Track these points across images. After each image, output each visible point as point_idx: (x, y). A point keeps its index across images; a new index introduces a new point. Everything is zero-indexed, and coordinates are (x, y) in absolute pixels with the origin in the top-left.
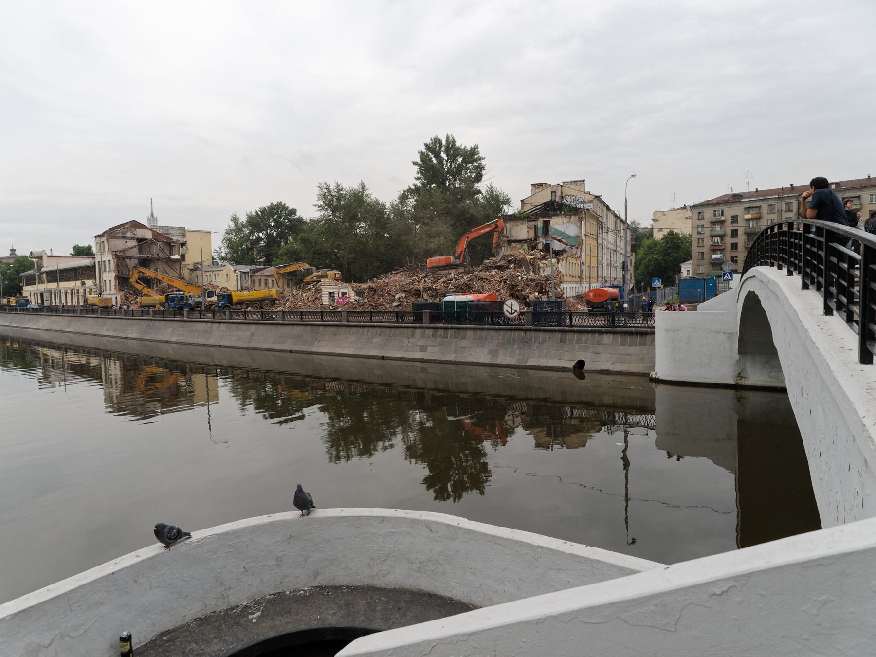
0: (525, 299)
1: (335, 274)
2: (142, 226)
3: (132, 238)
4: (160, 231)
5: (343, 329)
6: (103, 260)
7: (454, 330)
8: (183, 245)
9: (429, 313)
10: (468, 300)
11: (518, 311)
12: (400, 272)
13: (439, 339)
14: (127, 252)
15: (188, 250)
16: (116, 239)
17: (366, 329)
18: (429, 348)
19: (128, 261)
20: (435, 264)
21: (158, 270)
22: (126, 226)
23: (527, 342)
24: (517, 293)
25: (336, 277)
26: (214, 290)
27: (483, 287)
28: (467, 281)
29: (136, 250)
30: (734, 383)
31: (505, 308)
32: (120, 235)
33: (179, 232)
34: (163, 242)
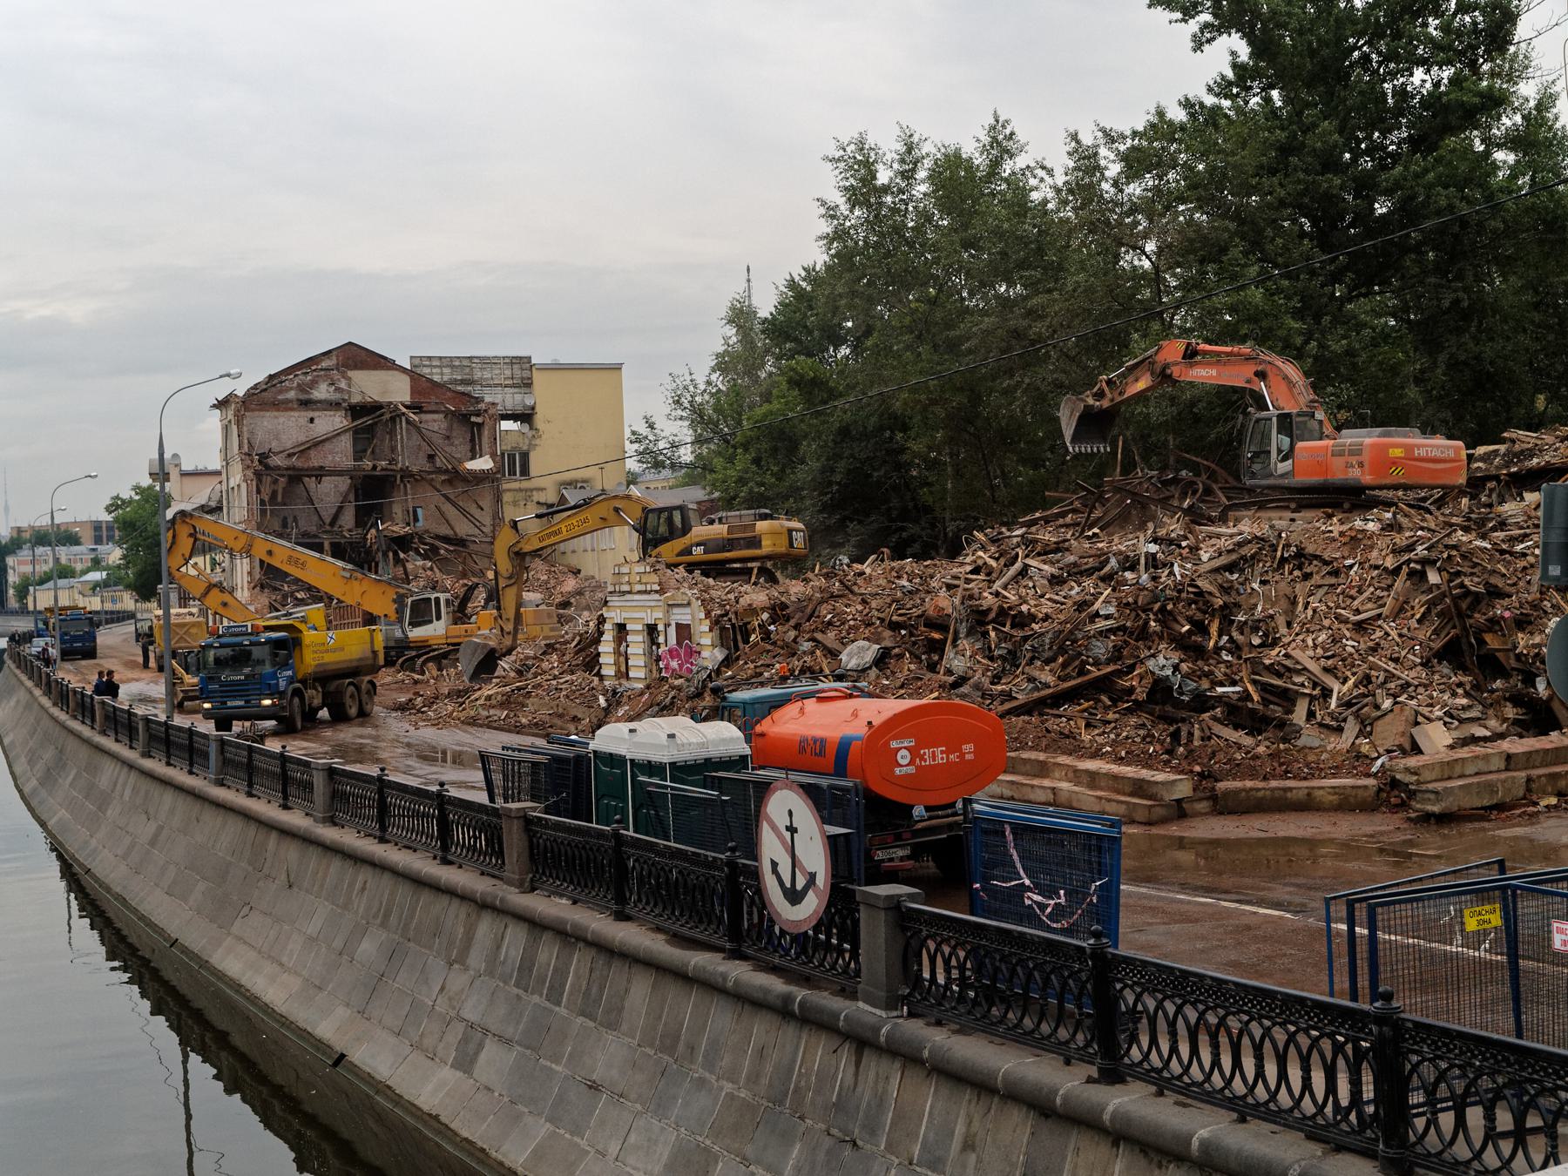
0: (1530, 680)
1: (790, 531)
2: (378, 362)
3: (333, 405)
4: (442, 374)
6: (231, 485)
7: (593, 952)
8: (526, 417)
9: (528, 822)
10: (641, 755)
11: (821, 881)
12: (1063, 515)
13: (536, 999)
14: (312, 453)
17: (365, 874)
19: (311, 483)
21: (419, 511)
22: (324, 365)
23: (855, 1144)
24: (1488, 638)
26: (433, 597)
27: (1293, 602)
28: (1216, 570)
29: (346, 443)
31: (771, 847)
32: (292, 395)
33: (508, 373)
34: (447, 413)
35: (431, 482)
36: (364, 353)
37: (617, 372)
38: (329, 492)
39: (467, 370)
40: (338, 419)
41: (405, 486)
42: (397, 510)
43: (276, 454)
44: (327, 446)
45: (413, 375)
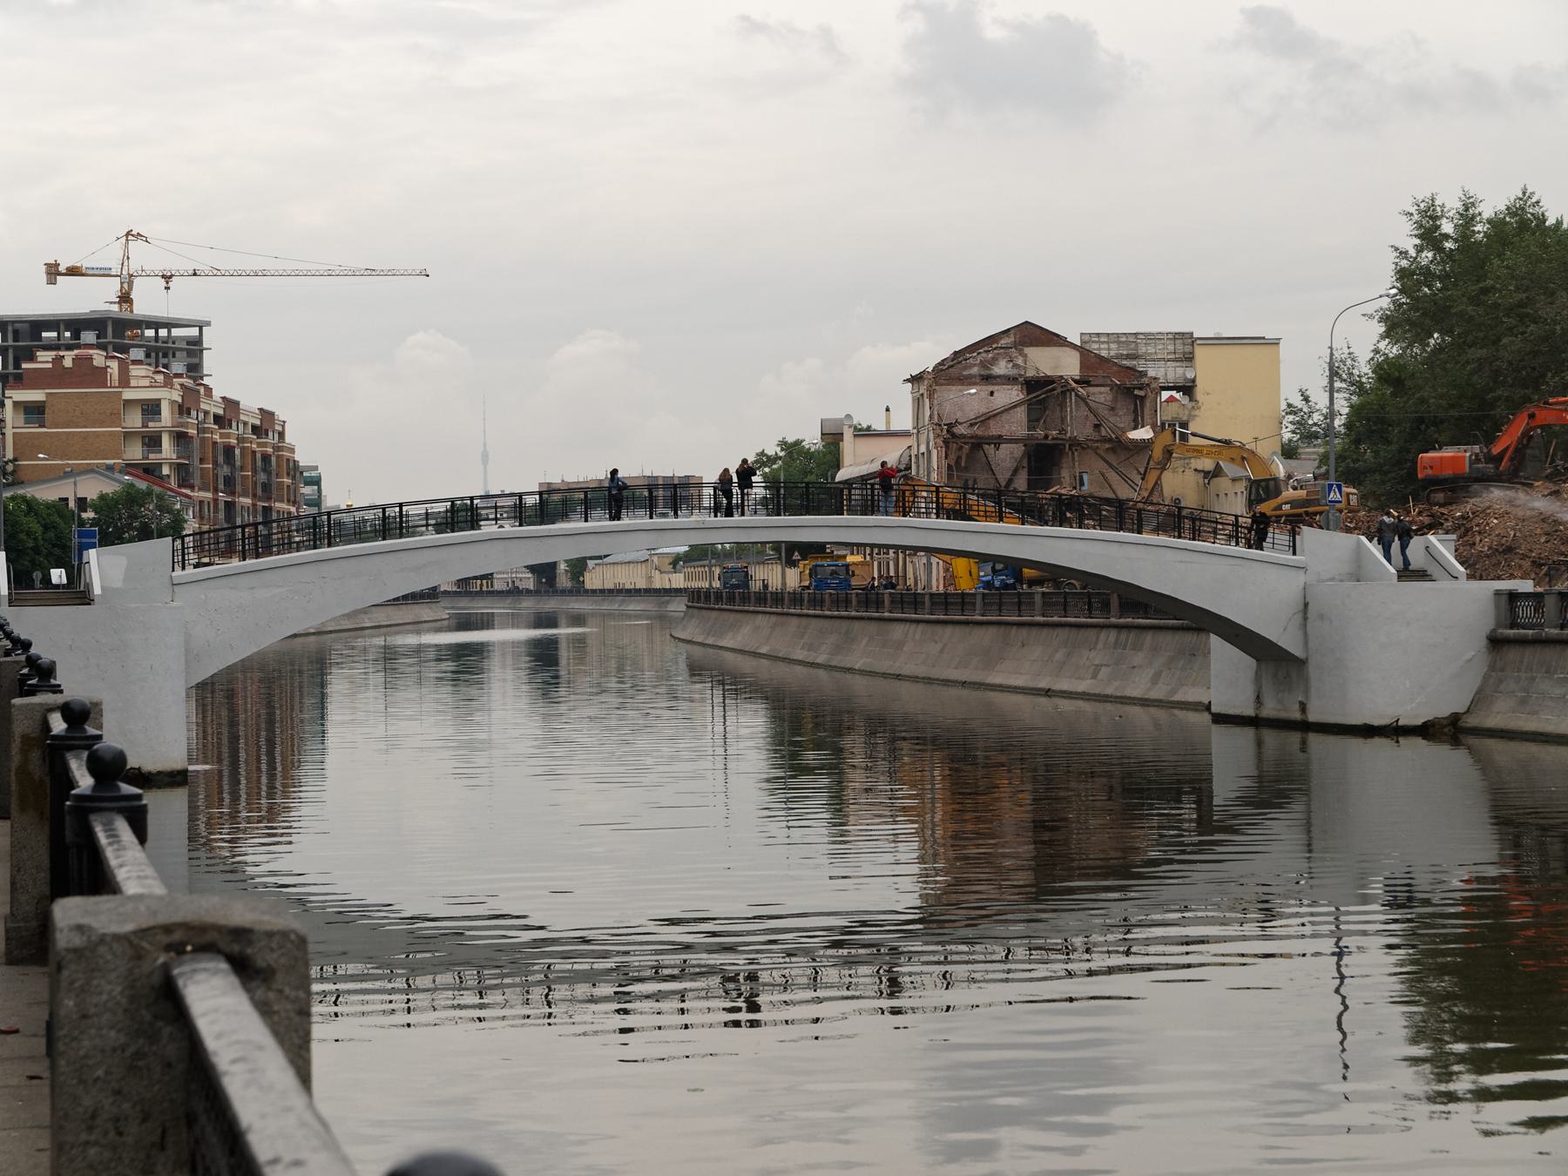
3: (1010, 380)
5: (1034, 631)
6: (921, 451)
14: (992, 422)
15: (1199, 408)
16: (963, 384)
18: (1104, 672)
19: (990, 449)
20: (1430, 472)
21: (1085, 477)
22: (1004, 342)
25: (1349, 504)
29: (1021, 414)
30: (1254, 715)
32: (975, 370)
33: (1171, 348)
34: (1112, 386)
35: (1095, 450)
36: (1038, 331)
37: (1275, 346)
38: (1005, 458)
39: (1133, 345)
40: (1015, 393)
41: (1073, 454)
42: (1065, 473)
43: (960, 424)
44: (1005, 416)
45: (1083, 351)
